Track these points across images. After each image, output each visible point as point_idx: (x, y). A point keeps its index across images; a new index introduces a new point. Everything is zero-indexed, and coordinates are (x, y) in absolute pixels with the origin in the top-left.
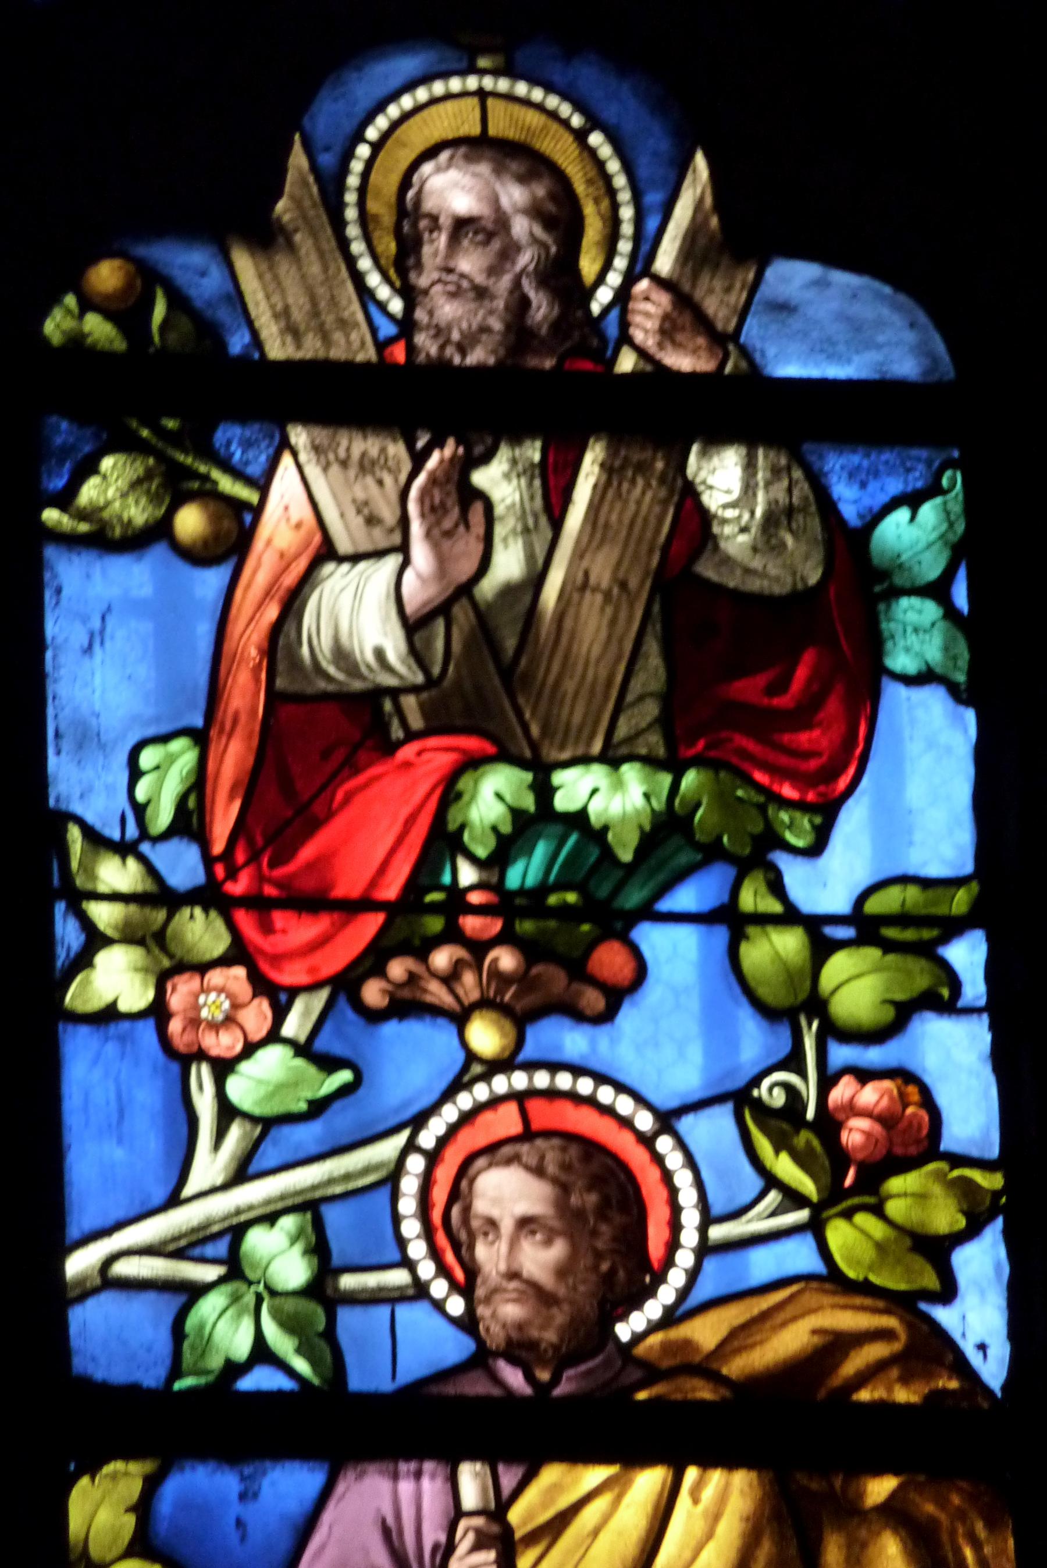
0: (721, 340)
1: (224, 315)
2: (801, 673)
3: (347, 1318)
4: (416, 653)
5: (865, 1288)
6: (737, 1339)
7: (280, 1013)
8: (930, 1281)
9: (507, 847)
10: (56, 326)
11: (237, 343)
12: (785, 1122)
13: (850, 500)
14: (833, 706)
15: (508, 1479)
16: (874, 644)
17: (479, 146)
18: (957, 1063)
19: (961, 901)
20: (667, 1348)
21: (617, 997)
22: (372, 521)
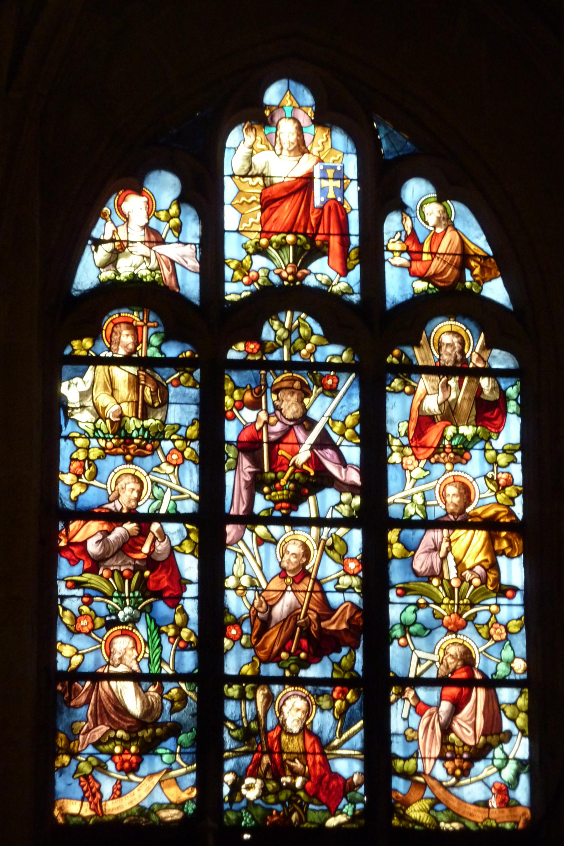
0: (485, 362)
1: (413, 358)
2: (496, 412)
3: (428, 508)
4: (440, 409)
5: (502, 504)
6: (484, 512)
7: (419, 463)
8: (512, 503)
9: (452, 439)
10: (388, 360)
11: (415, 362)
12: (491, 480)
13: (503, 386)
14: (500, 418)
15: (451, 532)
16: (506, 408)
17: (451, 332)
18: (517, 472)
19: (518, 447)
20: (474, 513)
21: (467, 461)
22: (434, 389)
